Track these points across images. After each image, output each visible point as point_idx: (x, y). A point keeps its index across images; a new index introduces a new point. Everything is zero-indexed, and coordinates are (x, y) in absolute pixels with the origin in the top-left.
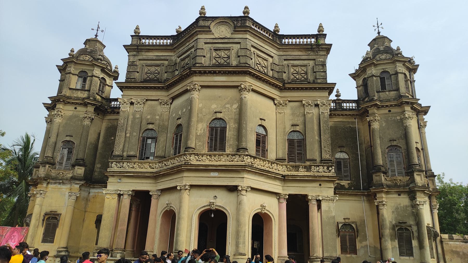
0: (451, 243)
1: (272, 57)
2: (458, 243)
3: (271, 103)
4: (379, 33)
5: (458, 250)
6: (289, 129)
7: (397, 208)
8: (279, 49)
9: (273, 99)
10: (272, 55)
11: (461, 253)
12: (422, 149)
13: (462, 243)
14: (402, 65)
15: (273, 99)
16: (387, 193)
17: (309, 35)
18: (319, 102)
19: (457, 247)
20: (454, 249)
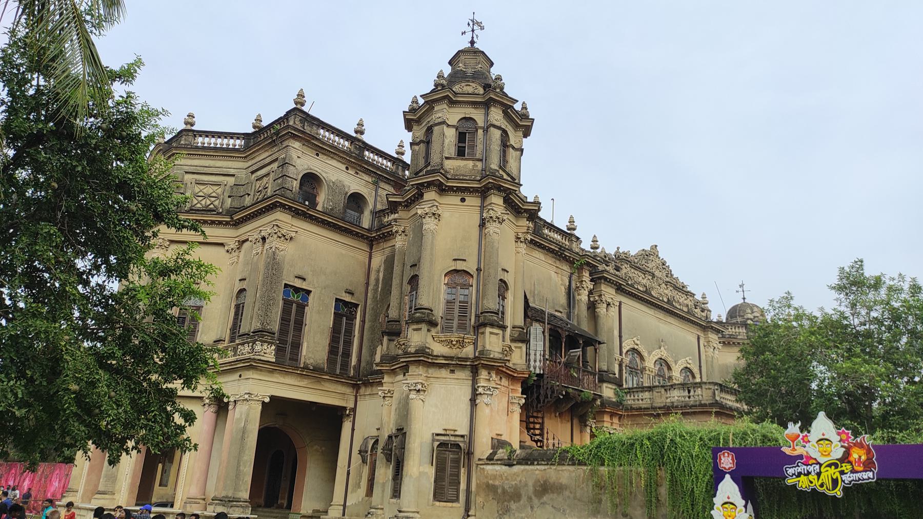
0: (489, 467)
1: (233, 175)
2: (497, 468)
3: (221, 250)
4: (472, 42)
5: (497, 483)
6: (238, 286)
7: (400, 403)
8: (245, 157)
9: (222, 245)
10: (232, 171)
11: (500, 491)
12: (479, 270)
13: (504, 467)
14: (445, 106)
15: (222, 245)
16: (393, 372)
17: (281, 118)
18: (263, 234)
19: (494, 477)
20: (491, 482)
